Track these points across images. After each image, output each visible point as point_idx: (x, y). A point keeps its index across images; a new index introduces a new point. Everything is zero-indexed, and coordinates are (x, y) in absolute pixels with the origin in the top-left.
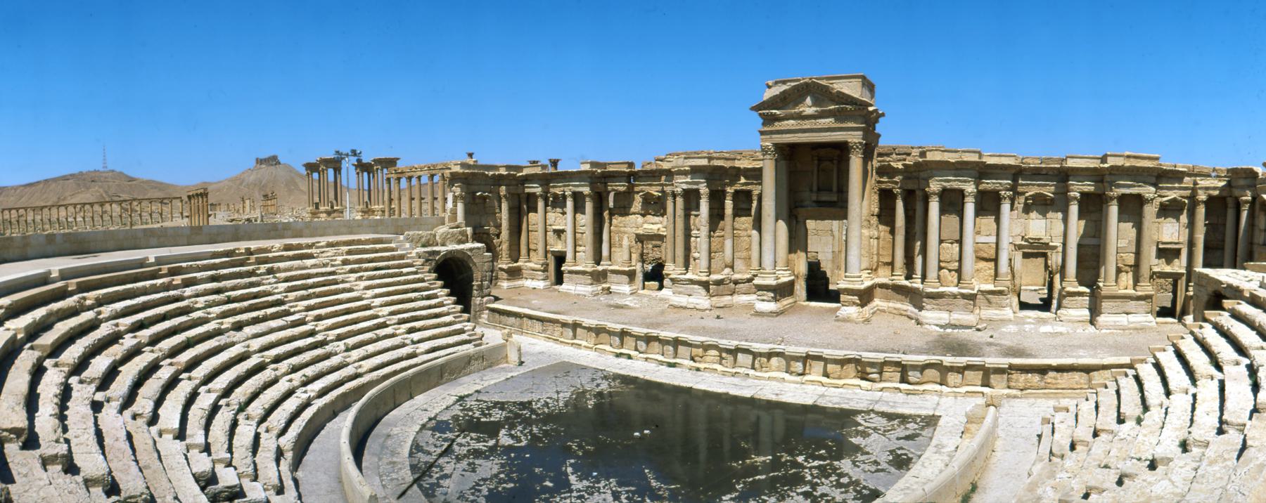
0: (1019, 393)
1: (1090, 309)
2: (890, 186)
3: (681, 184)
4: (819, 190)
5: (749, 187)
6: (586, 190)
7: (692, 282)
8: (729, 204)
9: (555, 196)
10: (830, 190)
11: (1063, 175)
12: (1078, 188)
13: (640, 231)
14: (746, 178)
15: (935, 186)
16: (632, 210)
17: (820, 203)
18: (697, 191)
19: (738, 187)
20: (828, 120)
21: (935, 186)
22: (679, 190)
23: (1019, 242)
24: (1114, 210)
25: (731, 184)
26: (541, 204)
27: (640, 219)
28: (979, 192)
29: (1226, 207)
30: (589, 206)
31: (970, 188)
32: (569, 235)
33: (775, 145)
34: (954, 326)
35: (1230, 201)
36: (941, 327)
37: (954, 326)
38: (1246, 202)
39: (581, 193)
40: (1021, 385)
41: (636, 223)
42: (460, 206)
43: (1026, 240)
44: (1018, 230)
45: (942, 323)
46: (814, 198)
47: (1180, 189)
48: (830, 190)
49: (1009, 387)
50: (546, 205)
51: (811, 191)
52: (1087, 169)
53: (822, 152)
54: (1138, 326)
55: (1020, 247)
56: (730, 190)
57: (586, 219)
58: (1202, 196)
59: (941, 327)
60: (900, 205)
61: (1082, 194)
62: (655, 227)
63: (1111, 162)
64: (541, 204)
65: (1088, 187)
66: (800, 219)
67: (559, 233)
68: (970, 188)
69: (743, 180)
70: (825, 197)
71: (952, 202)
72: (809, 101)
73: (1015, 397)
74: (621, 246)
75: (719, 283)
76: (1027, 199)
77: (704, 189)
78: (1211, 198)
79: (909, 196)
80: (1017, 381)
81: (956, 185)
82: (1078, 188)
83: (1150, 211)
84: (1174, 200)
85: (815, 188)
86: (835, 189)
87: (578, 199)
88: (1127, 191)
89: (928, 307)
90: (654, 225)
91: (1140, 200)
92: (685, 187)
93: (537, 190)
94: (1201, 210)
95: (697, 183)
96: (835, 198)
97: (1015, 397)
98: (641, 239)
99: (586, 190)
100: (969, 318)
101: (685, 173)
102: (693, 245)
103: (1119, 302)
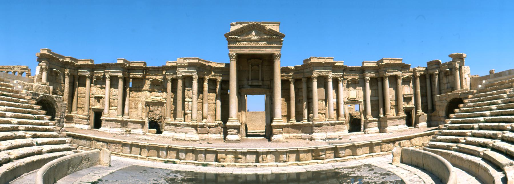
1: (378, 127)
2: (287, 77)
3: (182, 72)
4: (252, 80)
5: (216, 77)
6: (120, 75)
7: (188, 126)
8: (206, 86)
10: (258, 80)
11: (362, 70)
13: (149, 100)
14: (214, 72)
15: (315, 74)
16: (144, 88)
17: (251, 86)
19: (210, 77)
20: (264, 43)
21: (315, 74)
23: (346, 101)
25: (207, 75)
27: (148, 94)
30: (121, 84)
33: (237, 54)
35: (428, 76)
39: (117, 77)
41: (146, 95)
43: (349, 100)
44: (346, 96)
46: (250, 83)
48: (258, 80)
49: (381, 151)
50: (91, 83)
51: (248, 80)
53: (253, 61)
54: (402, 130)
56: (207, 78)
57: (118, 92)
61: (371, 78)
63: (385, 62)
66: (242, 94)
68: (330, 75)
69: (213, 73)
70: (255, 83)
72: (254, 33)
73: (385, 155)
74: (137, 108)
75: (202, 126)
76: (348, 81)
77: (195, 75)
79: (297, 82)
80: (385, 148)
82: (369, 75)
83: (400, 81)
85: (250, 79)
86: (260, 79)
89: (316, 131)
91: (396, 77)
92: (184, 74)
93: (87, 74)
94: (418, 80)
95: (192, 72)
96: (261, 84)
97: (385, 155)
98: (148, 104)
102: (186, 106)
103: (393, 121)
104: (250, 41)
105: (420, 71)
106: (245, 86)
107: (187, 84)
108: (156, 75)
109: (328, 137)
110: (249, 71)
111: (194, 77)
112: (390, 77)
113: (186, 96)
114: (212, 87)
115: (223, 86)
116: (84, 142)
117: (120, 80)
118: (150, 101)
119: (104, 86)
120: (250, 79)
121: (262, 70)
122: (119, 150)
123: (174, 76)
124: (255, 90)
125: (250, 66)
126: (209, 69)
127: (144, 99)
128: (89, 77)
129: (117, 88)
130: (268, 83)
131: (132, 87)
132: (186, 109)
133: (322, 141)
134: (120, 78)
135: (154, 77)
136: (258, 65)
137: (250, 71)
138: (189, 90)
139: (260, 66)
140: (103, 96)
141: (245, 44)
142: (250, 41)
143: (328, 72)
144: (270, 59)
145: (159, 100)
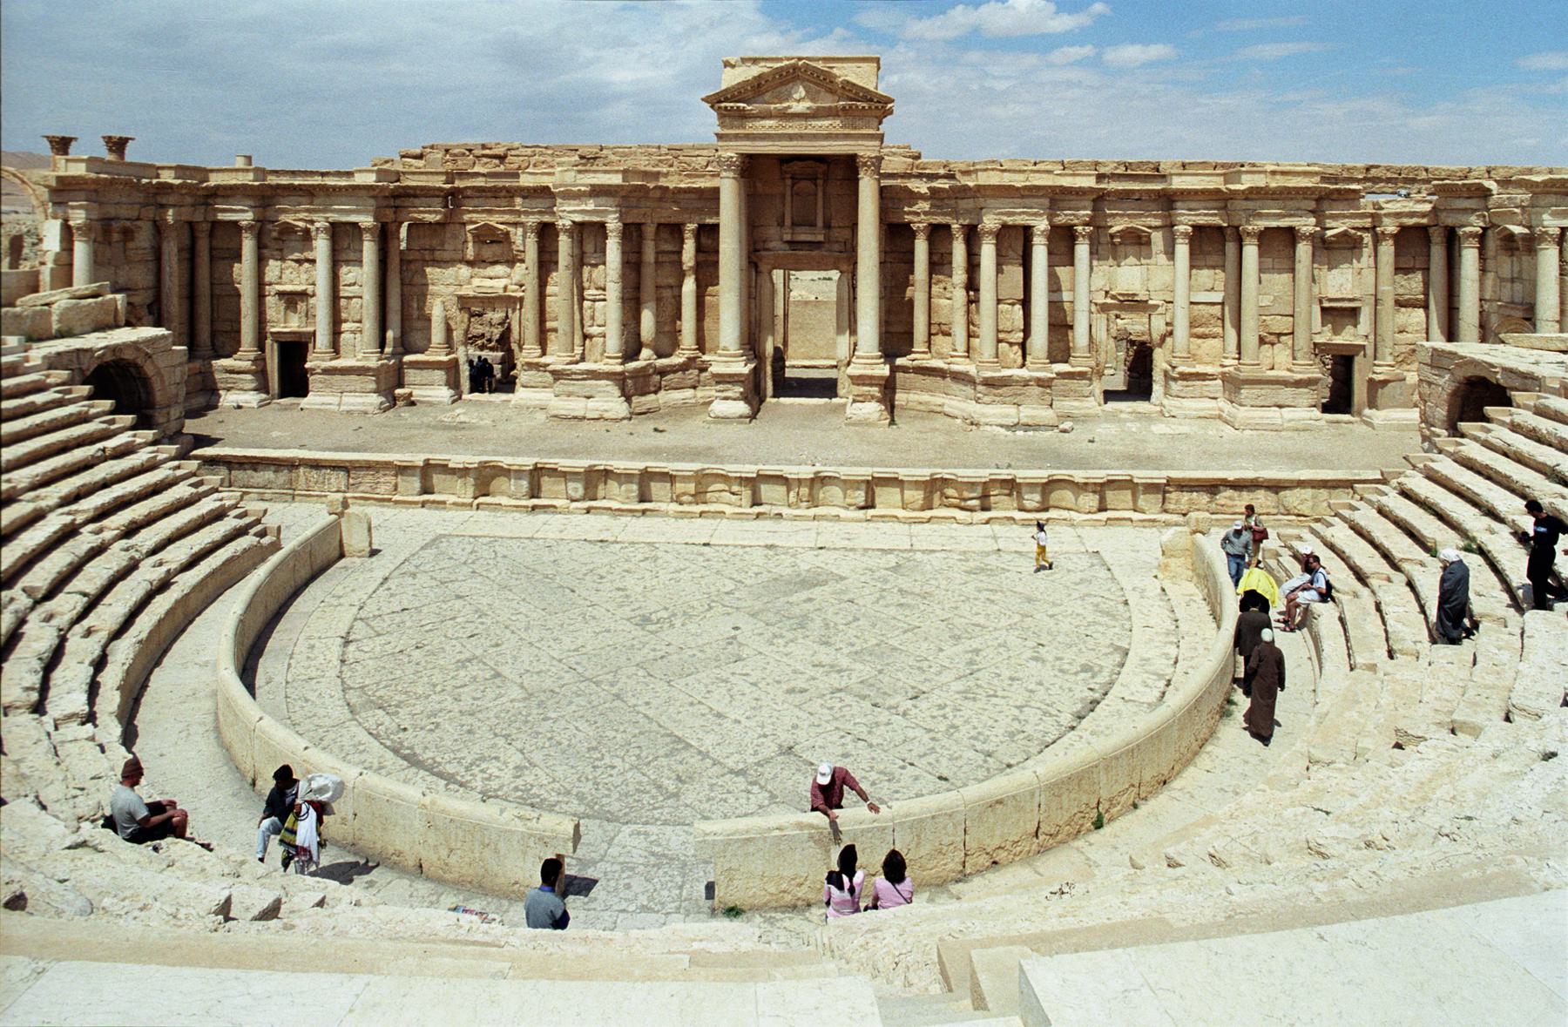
0: (1180, 519)
3: (568, 214)
6: (366, 220)
9: (288, 229)
10: (813, 225)
12: (1186, 220)
13: (467, 291)
18: (602, 225)
22: (564, 222)
23: (1101, 299)
24: (1251, 251)
26: (248, 245)
28: (1054, 227)
29: (1428, 242)
30: (369, 249)
31: (1041, 225)
32: (321, 303)
34: (1027, 427)
36: (1008, 427)
37: (1027, 427)
38: (1472, 235)
40: (1184, 508)
42: (81, 250)
43: (1113, 297)
44: (1099, 281)
45: (1010, 422)
46: (788, 237)
47: (1352, 216)
48: (813, 225)
49: (1166, 511)
51: (781, 224)
52: (1203, 192)
55: (1104, 308)
57: (361, 278)
58: (1390, 227)
59: (1008, 427)
60: (921, 248)
61: (1196, 227)
62: (498, 285)
64: (248, 245)
65: (1209, 217)
66: (763, 267)
67: (292, 299)
70: (804, 236)
71: (1015, 243)
77: (613, 223)
78: (1404, 229)
79: (939, 234)
80: (1177, 502)
81: (1020, 220)
83: (1304, 250)
84: (1345, 234)
85: (788, 222)
86: (820, 223)
87: (343, 238)
88: (1274, 224)
90: (496, 280)
91: (1291, 235)
92: (578, 218)
99: (366, 220)
100: (1046, 415)
101: (578, 196)
104: (785, 116)
105: (1398, 215)
106: (772, 245)
107: (589, 247)
108: (489, 212)
109: (1024, 420)
110: (783, 196)
111: (610, 226)
112: (1265, 237)
113: (586, 285)
114: (668, 247)
115: (704, 240)
116: (268, 475)
117: (367, 236)
118: (472, 294)
119: (309, 255)
120: (788, 222)
121: (824, 193)
122: (390, 487)
123: (547, 219)
124: (804, 255)
125: (789, 182)
126: (658, 194)
127: (451, 289)
128: (250, 228)
129: (359, 262)
130: (847, 233)
131: (408, 249)
132: (587, 322)
133: (1003, 431)
134: (368, 230)
135: (482, 219)
136: (814, 179)
137: (788, 198)
138: (596, 266)
139: (820, 182)
140: (310, 289)
141: (769, 125)
142: (785, 116)
143: (1035, 214)
144: (849, 165)
145: (501, 292)
